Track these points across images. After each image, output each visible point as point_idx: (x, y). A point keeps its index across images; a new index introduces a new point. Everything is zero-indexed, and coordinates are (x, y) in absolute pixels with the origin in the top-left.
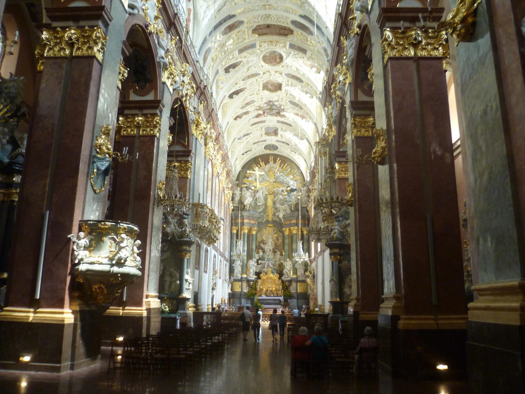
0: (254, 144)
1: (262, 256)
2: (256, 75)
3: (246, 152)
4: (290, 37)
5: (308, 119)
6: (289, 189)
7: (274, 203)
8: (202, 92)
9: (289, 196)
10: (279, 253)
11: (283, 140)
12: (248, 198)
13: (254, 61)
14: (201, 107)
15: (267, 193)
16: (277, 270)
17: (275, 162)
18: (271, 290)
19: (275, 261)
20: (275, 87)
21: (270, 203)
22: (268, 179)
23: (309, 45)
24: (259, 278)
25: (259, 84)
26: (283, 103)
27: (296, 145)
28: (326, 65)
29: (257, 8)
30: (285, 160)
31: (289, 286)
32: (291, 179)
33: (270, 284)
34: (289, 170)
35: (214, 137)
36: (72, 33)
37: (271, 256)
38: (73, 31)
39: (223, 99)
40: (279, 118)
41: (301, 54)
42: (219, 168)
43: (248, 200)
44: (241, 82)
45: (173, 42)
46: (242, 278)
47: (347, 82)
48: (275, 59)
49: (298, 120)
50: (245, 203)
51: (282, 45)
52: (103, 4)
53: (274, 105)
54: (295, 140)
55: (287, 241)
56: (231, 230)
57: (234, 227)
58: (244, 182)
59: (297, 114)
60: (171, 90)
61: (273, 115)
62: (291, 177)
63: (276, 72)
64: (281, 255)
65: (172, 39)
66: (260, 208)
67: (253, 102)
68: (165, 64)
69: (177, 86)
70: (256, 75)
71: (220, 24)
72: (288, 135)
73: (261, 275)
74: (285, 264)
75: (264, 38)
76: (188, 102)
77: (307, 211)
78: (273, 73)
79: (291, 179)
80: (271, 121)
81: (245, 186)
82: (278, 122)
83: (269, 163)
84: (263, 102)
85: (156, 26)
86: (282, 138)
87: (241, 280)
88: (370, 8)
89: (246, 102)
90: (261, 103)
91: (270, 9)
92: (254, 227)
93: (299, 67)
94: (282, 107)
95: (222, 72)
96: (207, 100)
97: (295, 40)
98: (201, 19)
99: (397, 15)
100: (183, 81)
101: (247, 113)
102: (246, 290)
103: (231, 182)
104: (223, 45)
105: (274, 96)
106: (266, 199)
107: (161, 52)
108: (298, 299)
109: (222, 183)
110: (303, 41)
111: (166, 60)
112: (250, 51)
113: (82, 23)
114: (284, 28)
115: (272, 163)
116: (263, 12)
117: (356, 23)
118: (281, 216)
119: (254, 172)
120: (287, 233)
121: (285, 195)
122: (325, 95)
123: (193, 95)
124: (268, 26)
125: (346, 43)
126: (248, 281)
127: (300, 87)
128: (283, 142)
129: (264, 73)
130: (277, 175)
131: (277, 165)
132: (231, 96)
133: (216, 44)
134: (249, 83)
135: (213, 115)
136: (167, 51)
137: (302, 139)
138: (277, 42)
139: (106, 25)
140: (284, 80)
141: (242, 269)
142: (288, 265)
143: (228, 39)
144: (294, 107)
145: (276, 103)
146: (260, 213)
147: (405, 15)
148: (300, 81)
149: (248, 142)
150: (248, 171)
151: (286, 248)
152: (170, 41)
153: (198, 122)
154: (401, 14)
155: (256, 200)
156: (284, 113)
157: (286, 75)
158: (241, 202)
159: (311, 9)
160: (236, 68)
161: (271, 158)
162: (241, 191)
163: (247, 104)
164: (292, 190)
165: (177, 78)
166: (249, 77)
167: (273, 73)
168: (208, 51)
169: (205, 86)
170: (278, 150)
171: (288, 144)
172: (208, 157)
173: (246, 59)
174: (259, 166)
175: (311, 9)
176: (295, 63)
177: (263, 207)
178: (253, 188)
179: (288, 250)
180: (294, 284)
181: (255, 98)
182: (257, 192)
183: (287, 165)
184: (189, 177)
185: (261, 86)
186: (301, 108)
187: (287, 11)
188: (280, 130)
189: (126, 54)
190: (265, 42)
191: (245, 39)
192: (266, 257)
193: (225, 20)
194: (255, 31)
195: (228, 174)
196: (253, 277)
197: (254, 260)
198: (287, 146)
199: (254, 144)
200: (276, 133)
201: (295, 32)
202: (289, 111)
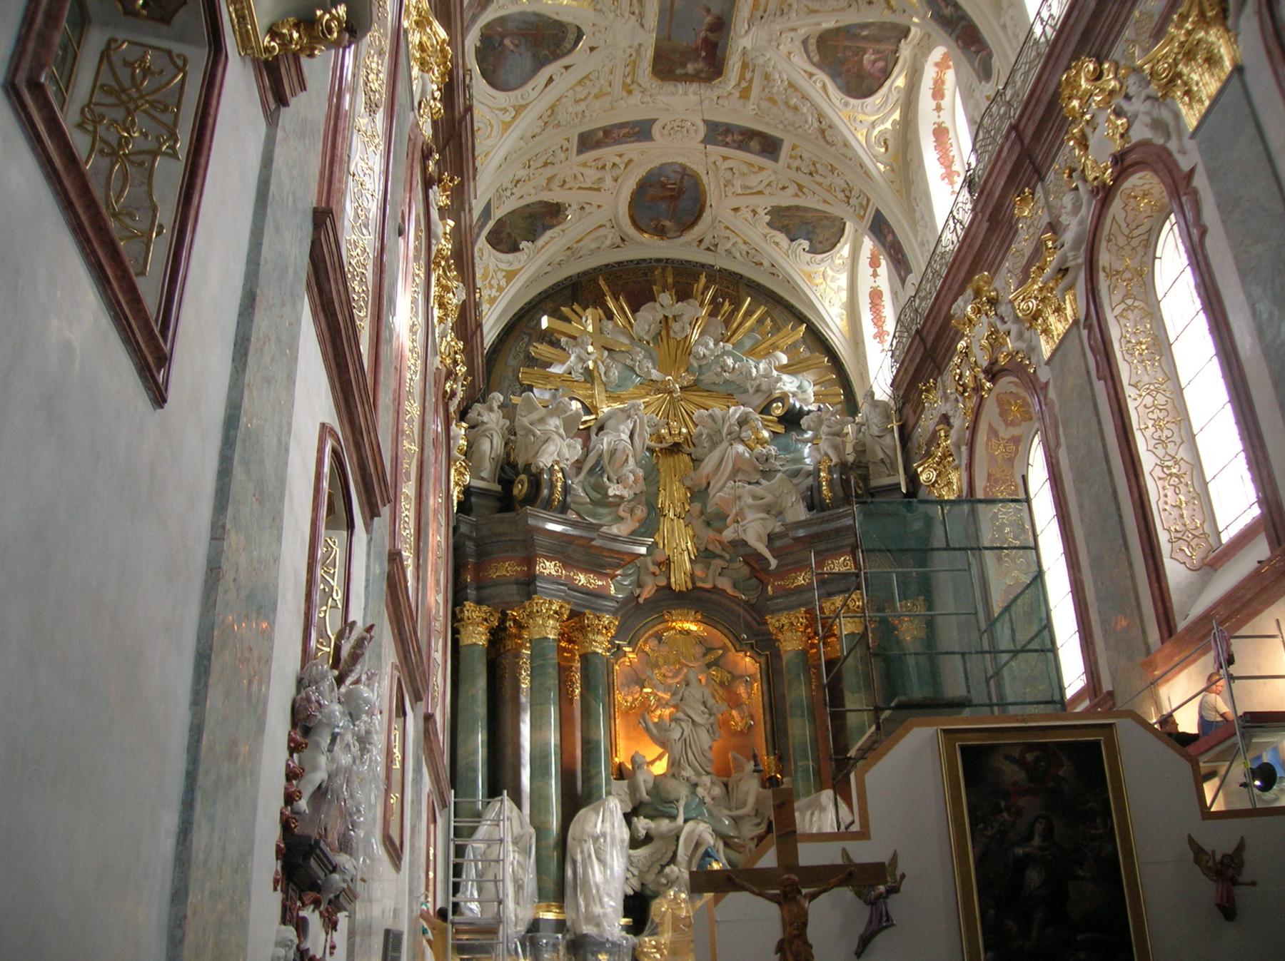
0: (587, 142)
6: (778, 409)
7: (699, 494)
9: (785, 449)
11: (745, 116)
19: (736, 820)
22: (655, 374)
27: (825, 131)
32: (783, 369)
37: (709, 789)
43: (556, 453)
56: (455, 631)
57: (471, 610)
62: (784, 359)
66: (622, 519)
79: (783, 369)
86: (745, 95)
92: (598, 611)
115: (665, 298)
120: (791, 644)
121: (762, 442)
130: (702, 350)
151: (799, 729)
155: (595, 469)
170: (707, 216)
171: (770, 147)
174: (601, 312)
179: (815, 742)
182: (601, 428)
199: (587, 142)
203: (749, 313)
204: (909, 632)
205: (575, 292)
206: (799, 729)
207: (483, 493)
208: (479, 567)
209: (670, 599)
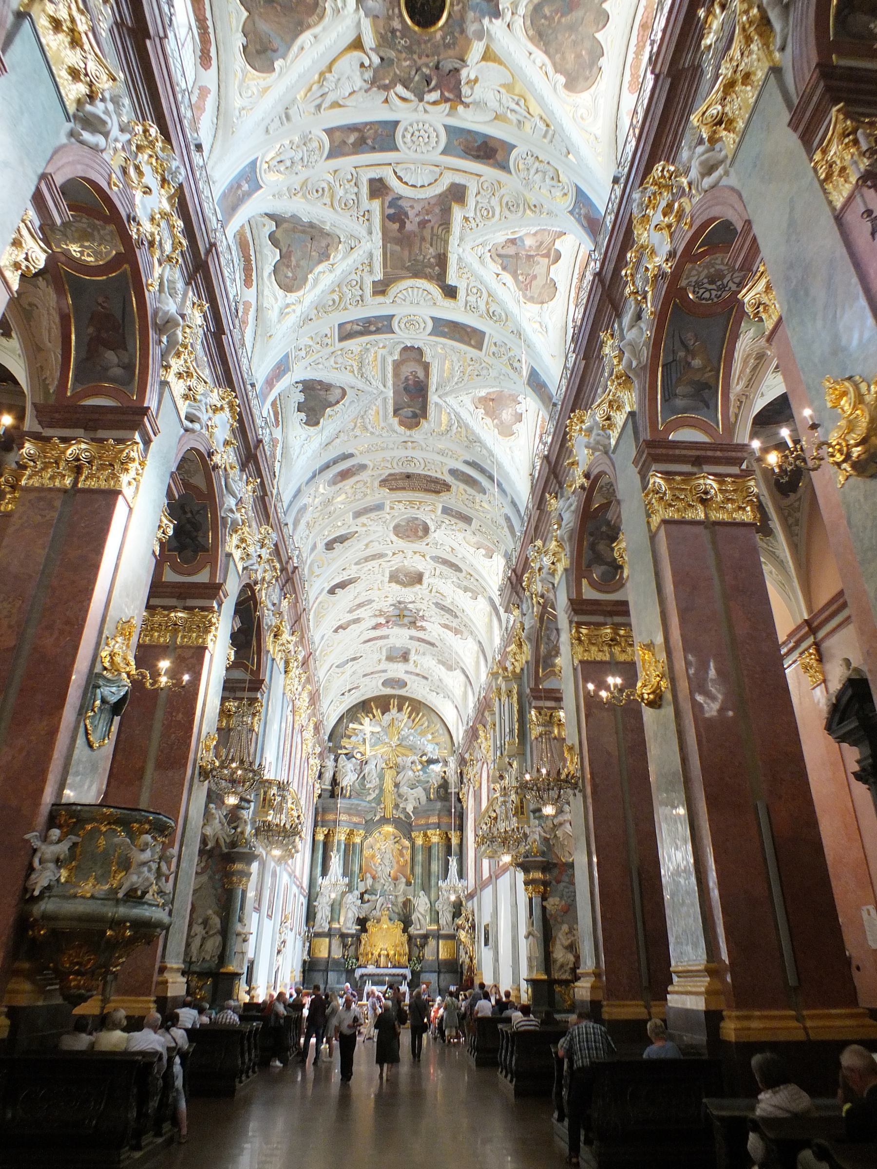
0: (364, 676)
1: (372, 886)
2: (381, 556)
3: (350, 691)
4: (445, 497)
5: (466, 634)
6: (424, 758)
7: (397, 785)
8: (289, 578)
9: (425, 772)
10: (404, 880)
11: (418, 671)
12: (350, 773)
13: (378, 532)
14: (285, 603)
15: (384, 765)
16: (399, 914)
17: (400, 709)
18: (388, 955)
19: (396, 896)
20: (411, 577)
21: (388, 785)
23: (477, 510)
24: (364, 930)
25: (383, 572)
26: (423, 607)
28: (510, 544)
29: (391, 445)
30: (417, 707)
31: (423, 946)
33: (385, 942)
34: (426, 724)
35: (300, 658)
36: (79, 449)
37: (389, 887)
38: (83, 446)
39: (320, 593)
40: (414, 632)
41: (462, 525)
42: (303, 718)
44: (353, 567)
45: (250, 488)
46: (330, 929)
47: (560, 568)
48: (415, 530)
49: (449, 635)
50: (344, 783)
51: (430, 508)
52: (145, 405)
53: (406, 608)
54: (441, 671)
55: (419, 858)
58: (343, 744)
59: (446, 626)
60: (240, 569)
61: (403, 625)
62: (430, 737)
63: (415, 553)
64: (408, 884)
65: (248, 483)
67: (370, 602)
68: (234, 522)
69: (251, 562)
70: (381, 556)
71: (327, 467)
72: (427, 662)
73: (368, 924)
74: (415, 901)
75: (400, 495)
76: (264, 592)
77: (459, 800)
78: (409, 554)
80: (400, 637)
81: (344, 751)
82: (411, 638)
83: (389, 710)
84: (388, 604)
85: (226, 457)
87: (329, 934)
88: (613, 442)
89: (357, 602)
90: (385, 605)
91: (414, 448)
93: (455, 545)
94: (421, 614)
95: (321, 546)
96: (295, 593)
97: (453, 501)
98: (295, 457)
99: (671, 452)
100: (260, 556)
101: (357, 621)
102: (337, 954)
103: (320, 743)
104: (329, 502)
105: (407, 594)
106: (381, 777)
107: (231, 502)
108: (439, 973)
109: (309, 744)
110: (467, 502)
111: (238, 515)
112: (373, 515)
113: (101, 434)
114: (436, 481)
115: (394, 711)
116: (402, 453)
117: (579, 471)
118: (410, 809)
119: (360, 727)
120: (419, 842)
122: (508, 591)
123: (274, 581)
124: (408, 476)
125: (554, 504)
126: (343, 936)
127: (455, 579)
128: (418, 675)
129: (394, 554)
131: (404, 716)
132: (332, 591)
133: (317, 500)
134: (366, 569)
135: (303, 619)
136: (240, 501)
137: (450, 668)
138: (420, 502)
139: (147, 442)
140: (429, 567)
141: (332, 911)
142: (421, 903)
143: (338, 493)
144: (443, 613)
145: (410, 606)
146: (369, 802)
147: (684, 452)
148: (458, 569)
149: (354, 673)
150: (351, 726)
151: (418, 870)
152: (244, 485)
153: (279, 629)
154: (677, 452)
156: (424, 624)
157: (432, 558)
158: (334, 782)
159: (484, 452)
160: (345, 544)
161: (394, 702)
162: (336, 761)
163: (360, 606)
164: (431, 762)
165: (251, 550)
166: (367, 559)
167: (409, 554)
168: (304, 508)
169: (296, 568)
172: (289, 694)
173: (365, 529)
175: (484, 452)
176: (447, 538)
177: (377, 792)
178: (358, 756)
180: (432, 942)
181: (374, 595)
183: (423, 716)
184: (256, 729)
185: (387, 575)
186: (456, 617)
187: (441, 453)
188: (413, 652)
189: (173, 495)
190: (399, 502)
191: (365, 495)
192: (378, 887)
193: (335, 462)
194: (384, 483)
195: (316, 728)
196: (353, 929)
197: (357, 893)
198: (425, 681)
199: (364, 676)
200: (405, 657)
201: (454, 489)
202: (432, 620)
203: (423, 716)
204: (455, 841)
205: (364, 707)
206: (418, 870)
207: (325, 790)
208: (323, 815)
209: (384, 820)
